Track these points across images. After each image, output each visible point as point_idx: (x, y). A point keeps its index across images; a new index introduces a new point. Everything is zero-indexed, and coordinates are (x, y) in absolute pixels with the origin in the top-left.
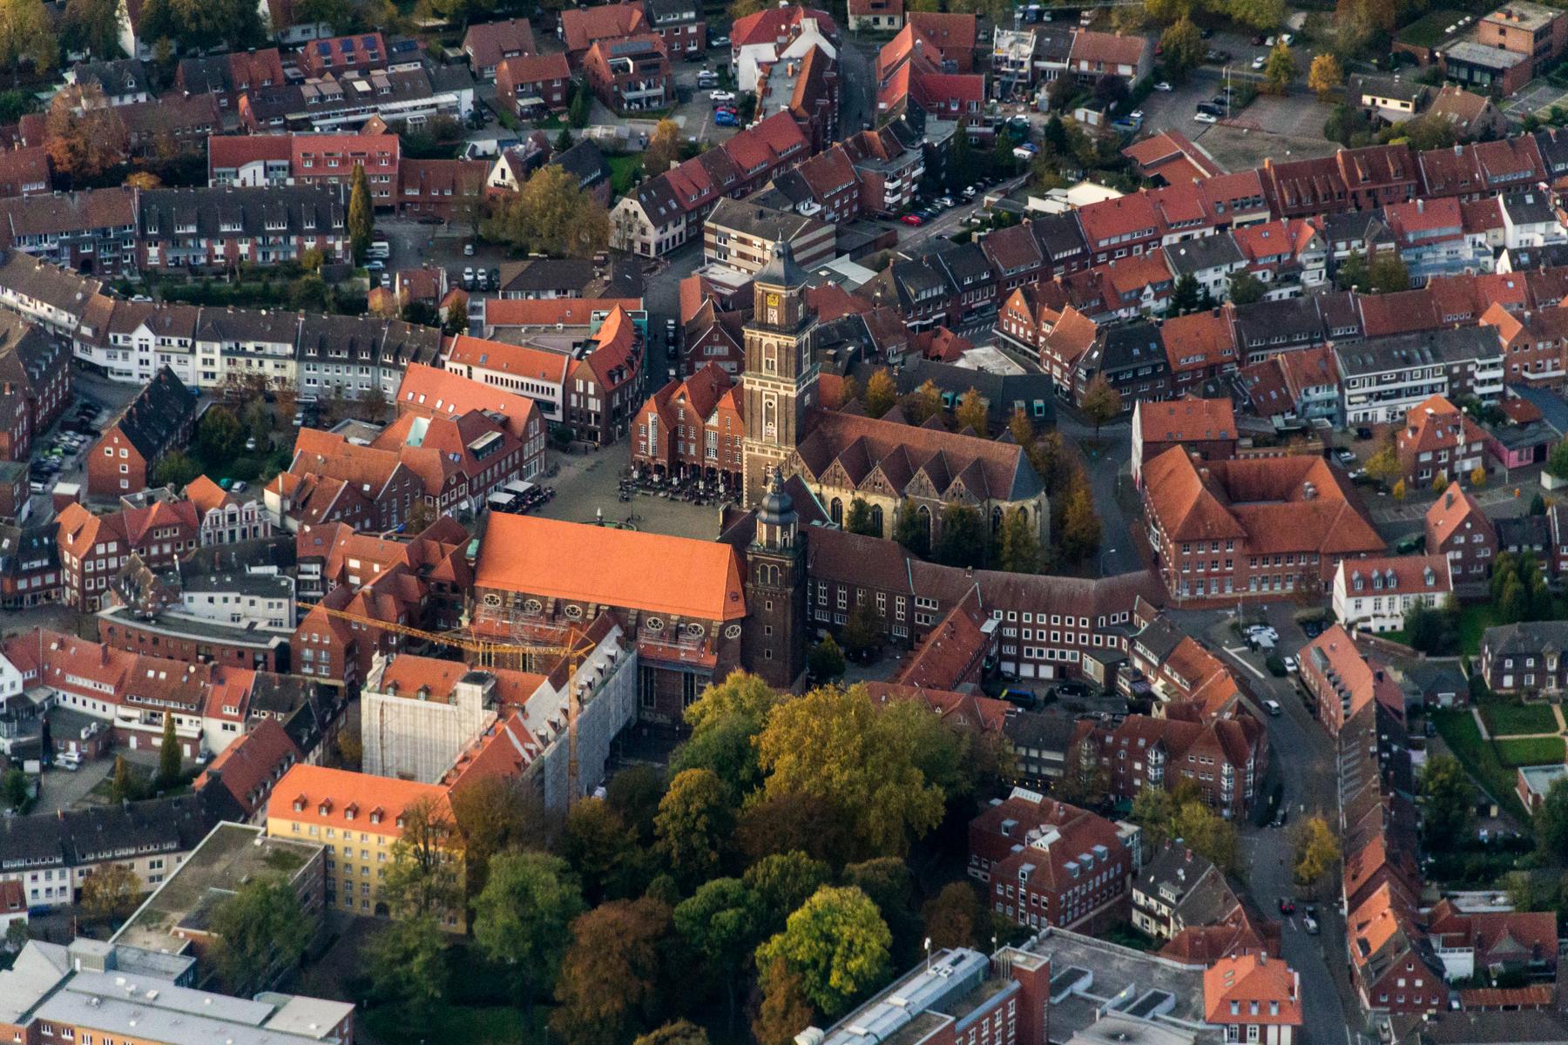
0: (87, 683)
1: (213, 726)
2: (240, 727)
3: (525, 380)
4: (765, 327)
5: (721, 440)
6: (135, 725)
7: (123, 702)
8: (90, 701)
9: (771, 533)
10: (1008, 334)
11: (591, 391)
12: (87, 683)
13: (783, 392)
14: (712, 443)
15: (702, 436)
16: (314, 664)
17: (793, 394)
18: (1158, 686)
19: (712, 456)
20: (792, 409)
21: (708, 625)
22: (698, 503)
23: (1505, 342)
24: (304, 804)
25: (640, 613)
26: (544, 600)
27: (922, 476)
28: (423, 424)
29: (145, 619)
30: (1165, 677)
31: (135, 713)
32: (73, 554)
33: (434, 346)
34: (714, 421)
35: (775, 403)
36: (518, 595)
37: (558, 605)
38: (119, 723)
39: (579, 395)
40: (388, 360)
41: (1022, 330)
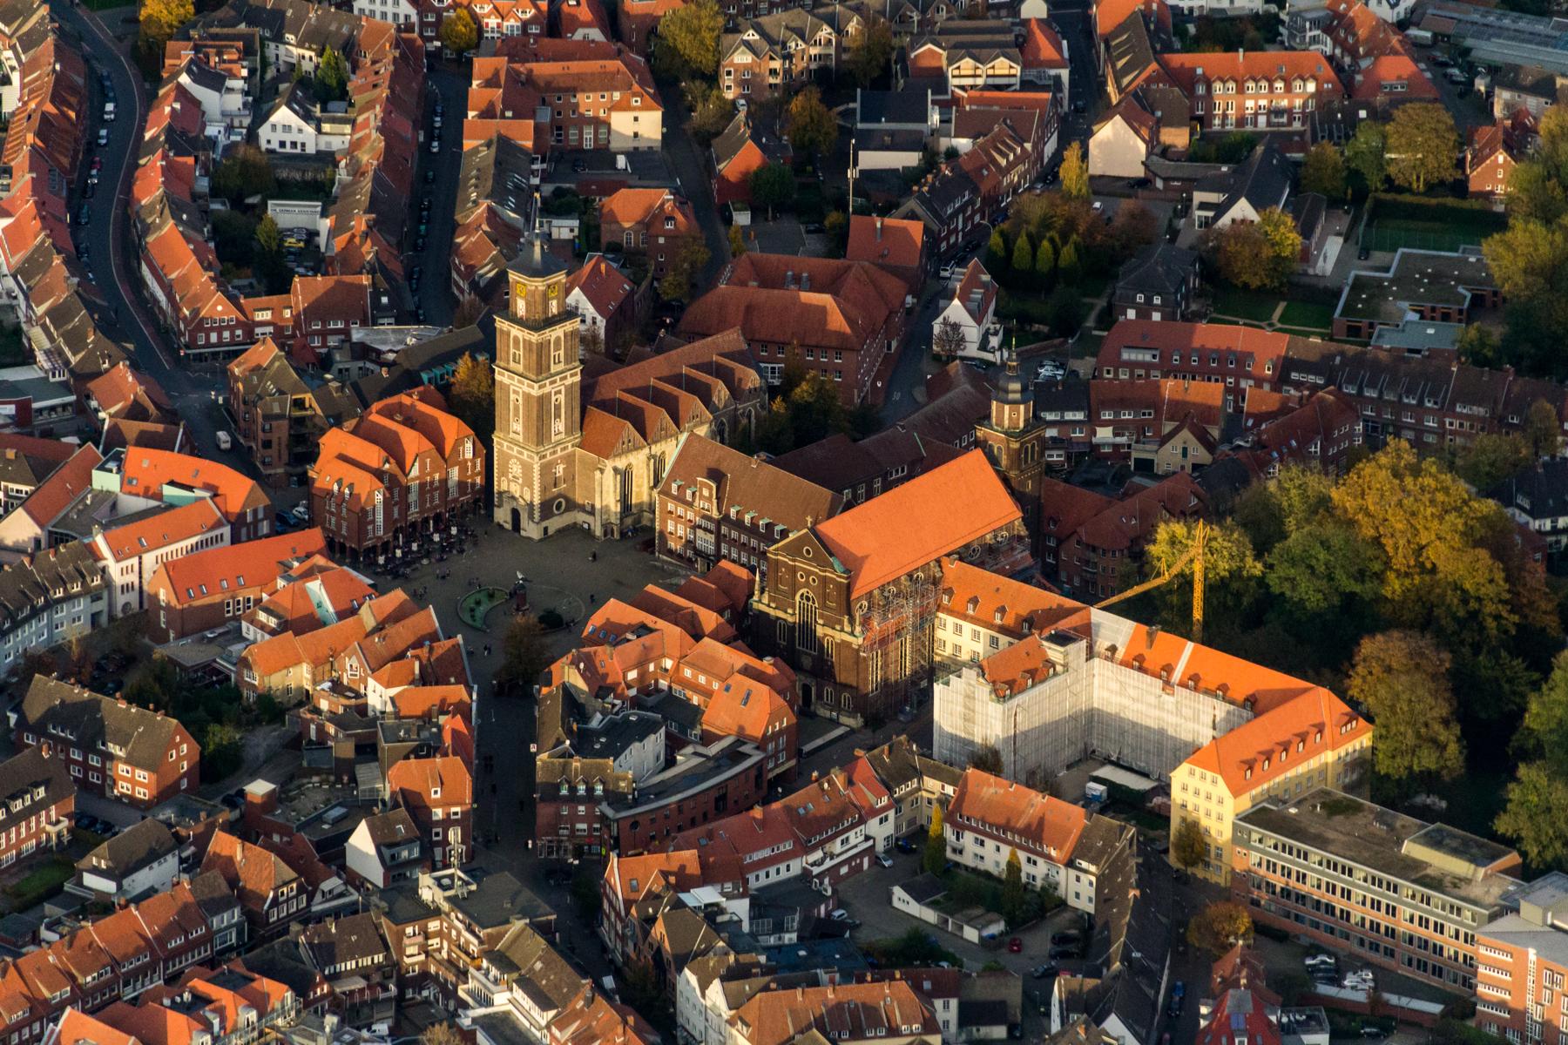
0: (766, 853)
1: (873, 827)
2: (891, 814)
3: (194, 540)
4: (550, 322)
5: (422, 486)
6: (828, 864)
7: (809, 850)
8: (772, 870)
9: (1027, 411)
10: (208, 344)
11: (261, 516)
12: (766, 853)
13: (569, 381)
14: (413, 497)
15: (408, 489)
16: (775, 756)
17: (578, 378)
18: (1104, 434)
19: (413, 510)
20: (577, 394)
21: (1009, 526)
22: (461, 551)
23: (529, 144)
24: (1250, 765)
25: (967, 546)
26: (896, 582)
27: (721, 393)
28: (315, 587)
29: (636, 803)
30: (1105, 424)
31: (818, 855)
32: (445, 803)
33: (85, 558)
34: (415, 472)
35: (562, 397)
36: (882, 588)
37: (910, 576)
38: (816, 870)
39: (248, 525)
40: (60, 594)
41: (226, 334)
